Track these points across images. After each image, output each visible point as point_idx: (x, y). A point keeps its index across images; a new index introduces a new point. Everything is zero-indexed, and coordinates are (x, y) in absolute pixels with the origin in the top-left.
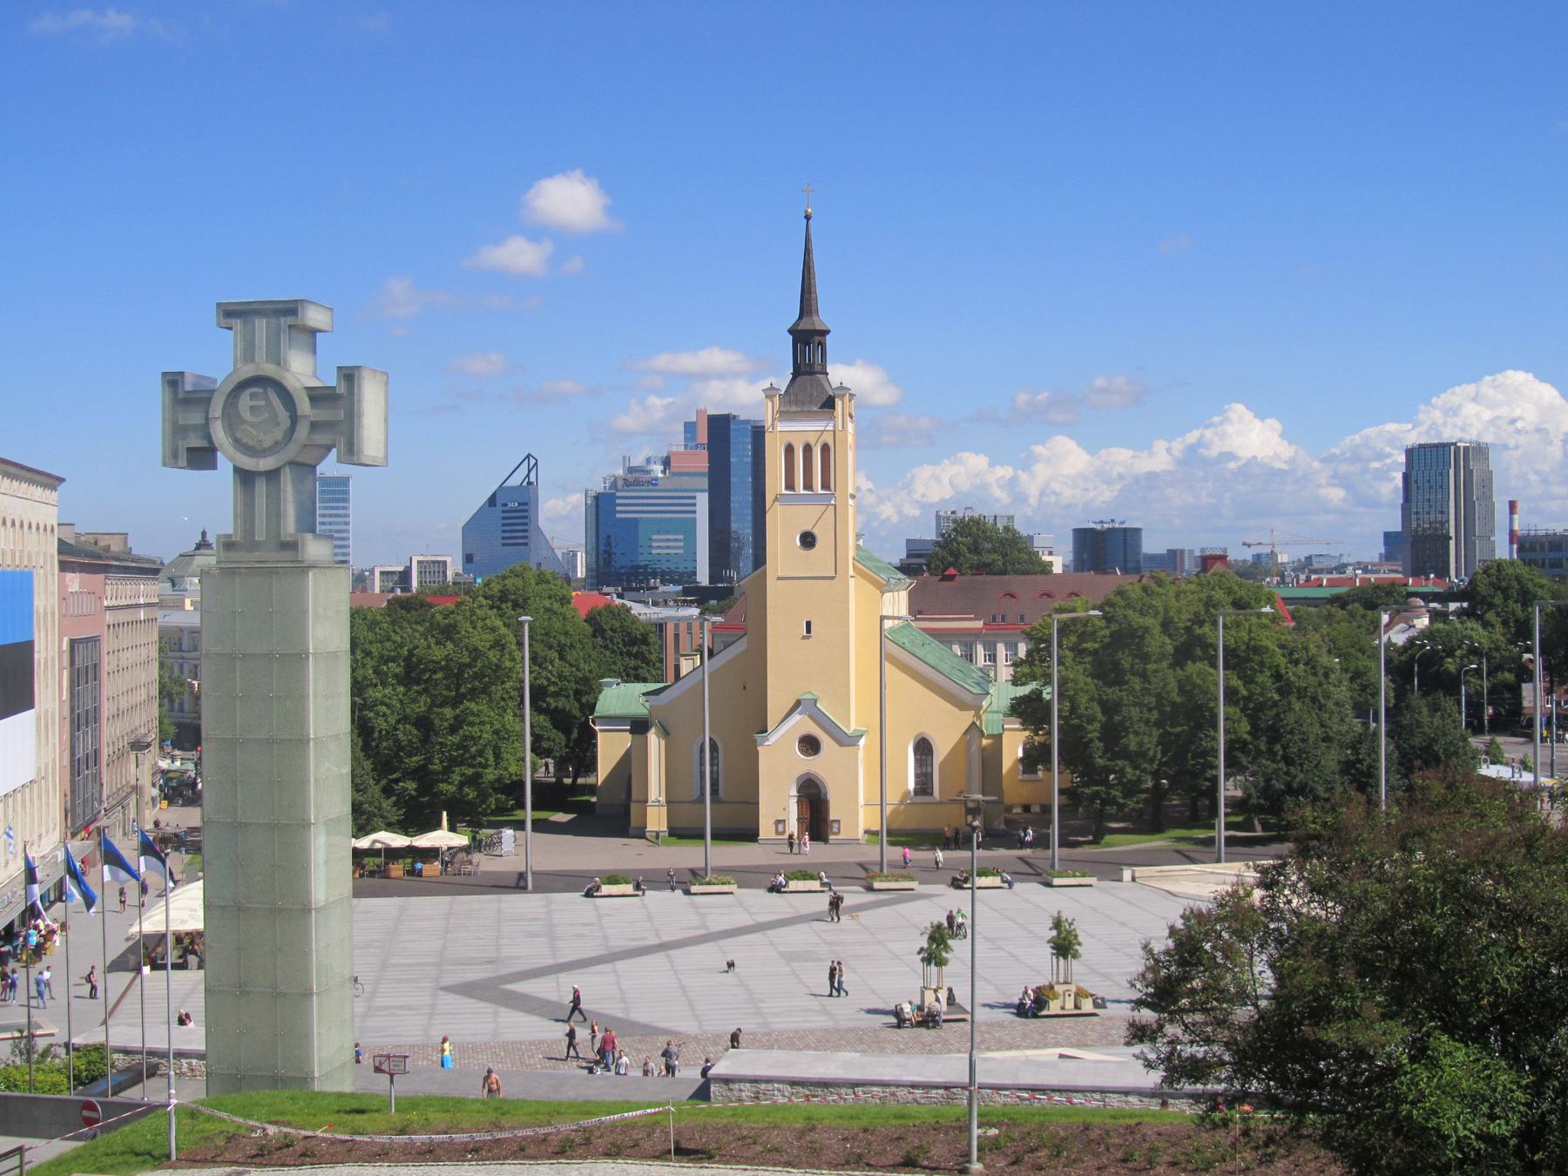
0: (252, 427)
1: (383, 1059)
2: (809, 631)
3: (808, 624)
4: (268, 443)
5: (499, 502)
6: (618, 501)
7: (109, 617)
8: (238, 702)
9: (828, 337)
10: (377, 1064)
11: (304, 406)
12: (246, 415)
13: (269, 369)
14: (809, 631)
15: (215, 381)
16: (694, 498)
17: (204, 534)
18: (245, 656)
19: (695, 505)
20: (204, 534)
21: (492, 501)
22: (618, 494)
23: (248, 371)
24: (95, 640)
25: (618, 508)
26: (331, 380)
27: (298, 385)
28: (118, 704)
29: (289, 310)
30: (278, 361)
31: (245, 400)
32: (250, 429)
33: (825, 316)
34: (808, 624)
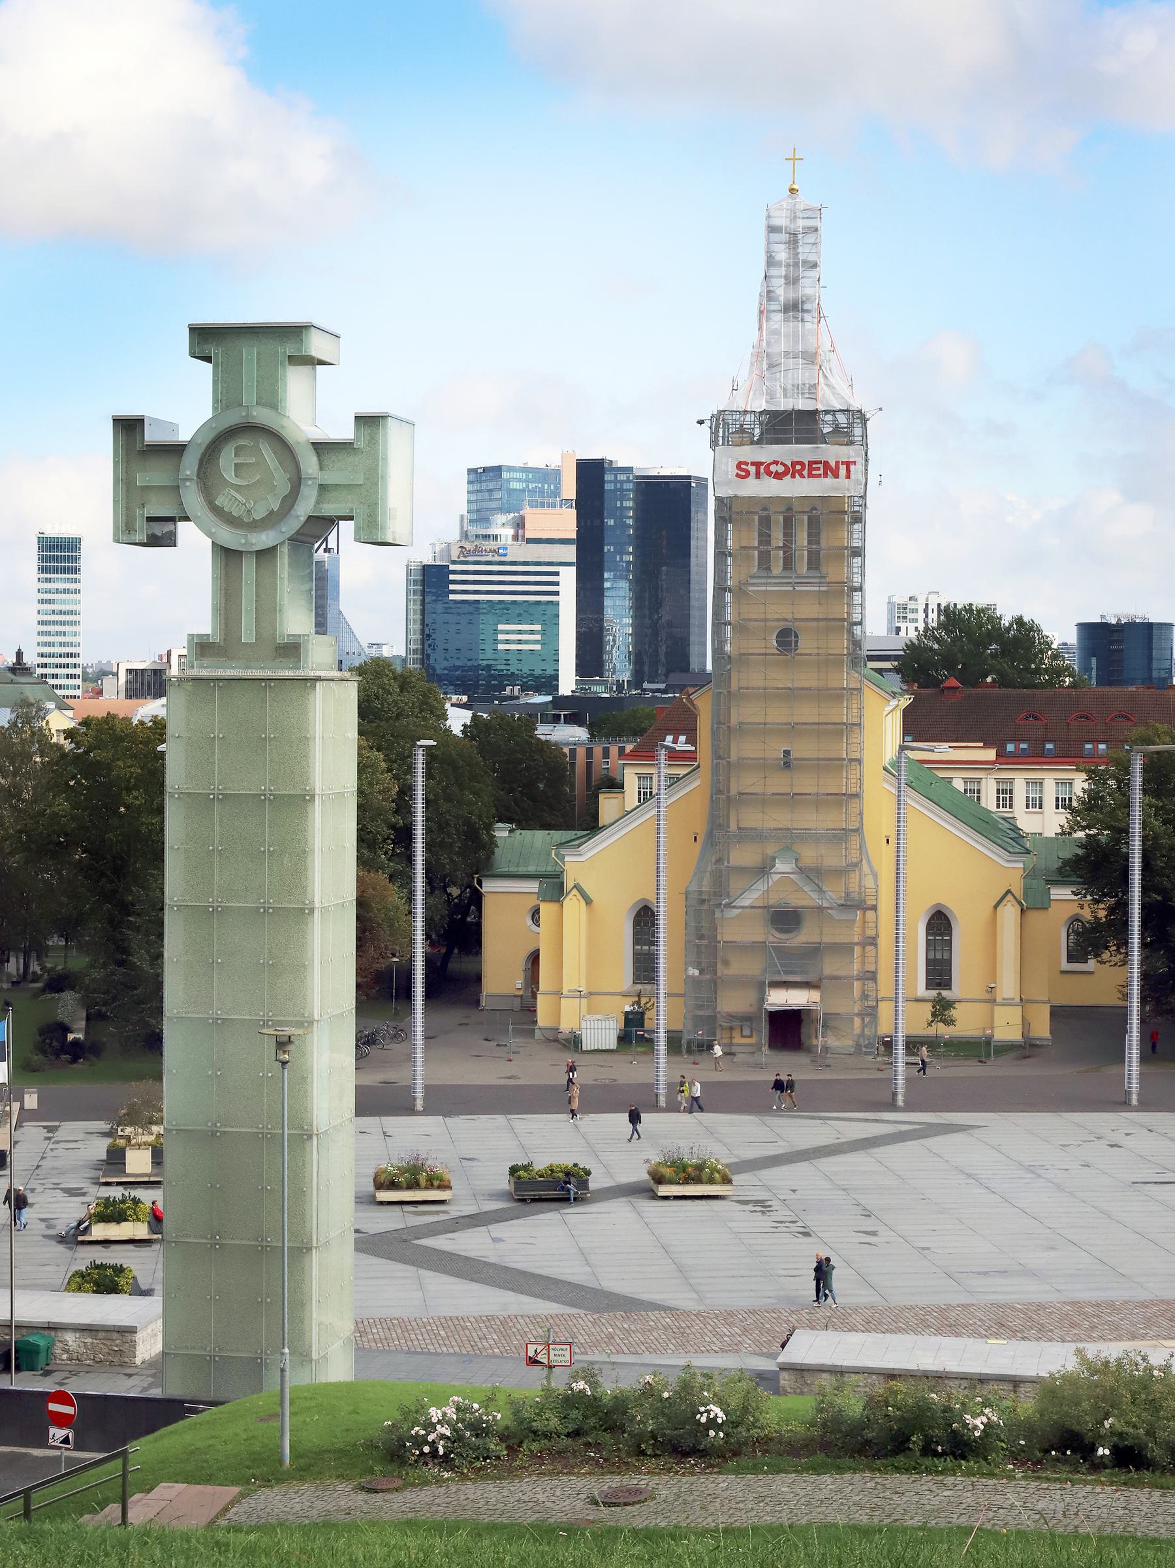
0: (237, 491)
1: (540, 1348)
4: (259, 514)
6: (452, 577)
8: (216, 858)
10: (531, 1354)
11: (310, 464)
12: (229, 475)
13: (261, 416)
15: (174, 427)
18: (226, 796)
22: (452, 567)
23: (233, 418)
25: (452, 587)
26: (344, 431)
27: (302, 439)
29: (295, 332)
30: (272, 401)
31: (227, 459)
32: (233, 493)
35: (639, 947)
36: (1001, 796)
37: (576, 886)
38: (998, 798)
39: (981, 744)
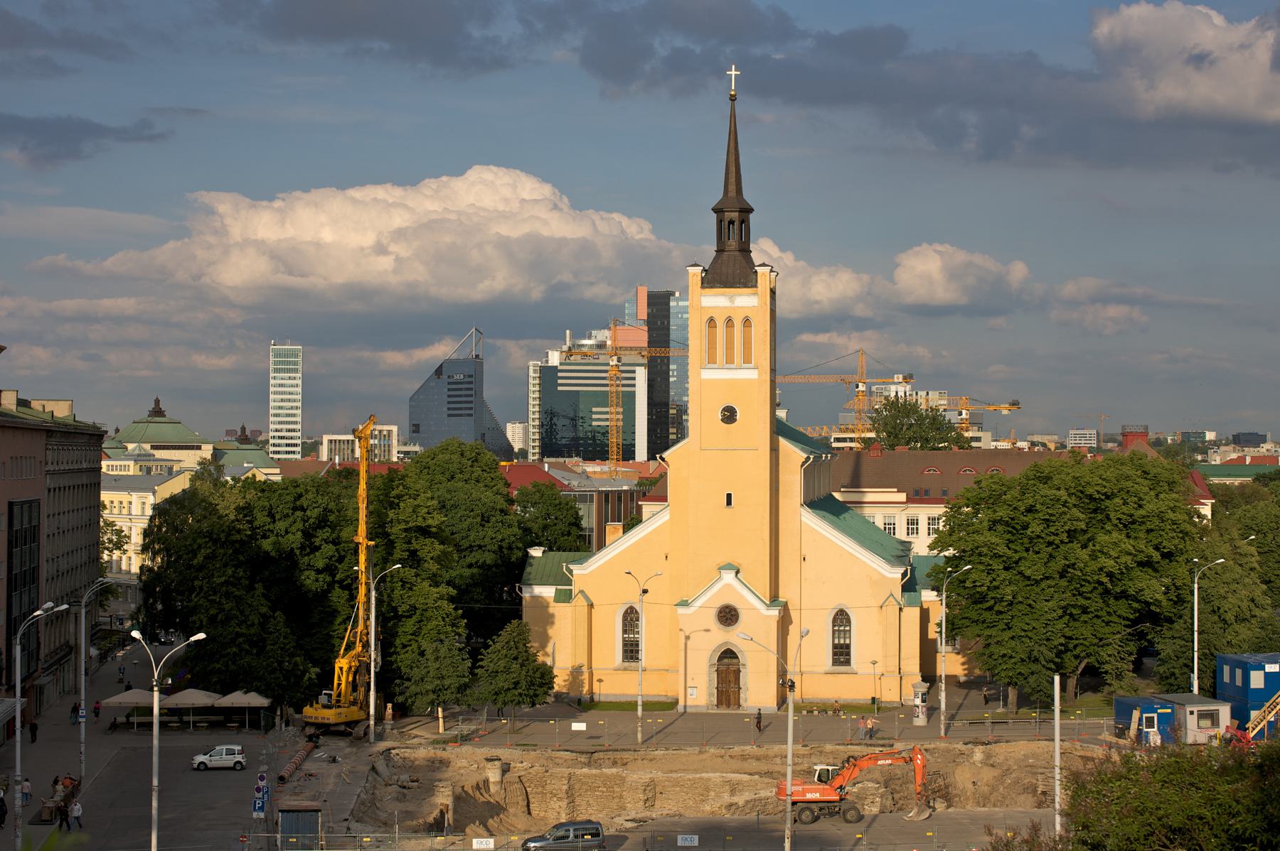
2: (729, 502)
3: (729, 496)
5: (445, 377)
6: (560, 374)
7: (49, 482)
9: (751, 216)
14: (729, 502)
16: (634, 372)
17: (157, 402)
19: (634, 379)
20: (157, 402)
21: (439, 372)
22: (560, 368)
24: (33, 505)
28: (58, 566)
33: (749, 196)
34: (729, 496)
35: (626, 636)
36: (910, 527)
37: (582, 592)
38: (908, 529)
39: (896, 490)
